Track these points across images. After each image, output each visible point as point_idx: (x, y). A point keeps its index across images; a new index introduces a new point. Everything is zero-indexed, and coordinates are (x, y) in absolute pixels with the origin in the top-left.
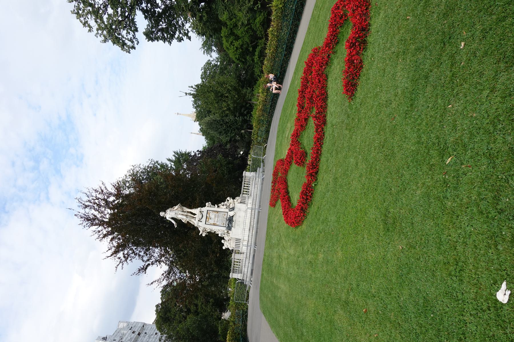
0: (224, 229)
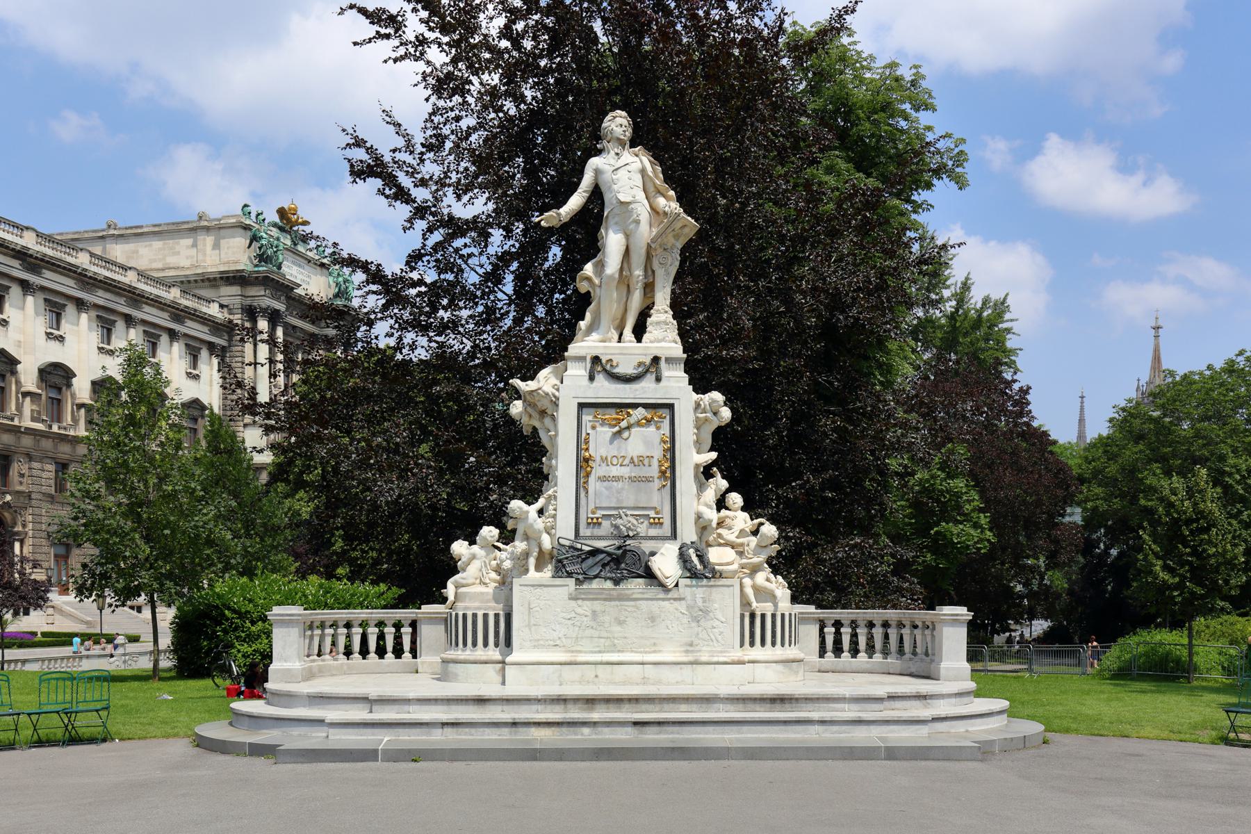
0: (565, 530)
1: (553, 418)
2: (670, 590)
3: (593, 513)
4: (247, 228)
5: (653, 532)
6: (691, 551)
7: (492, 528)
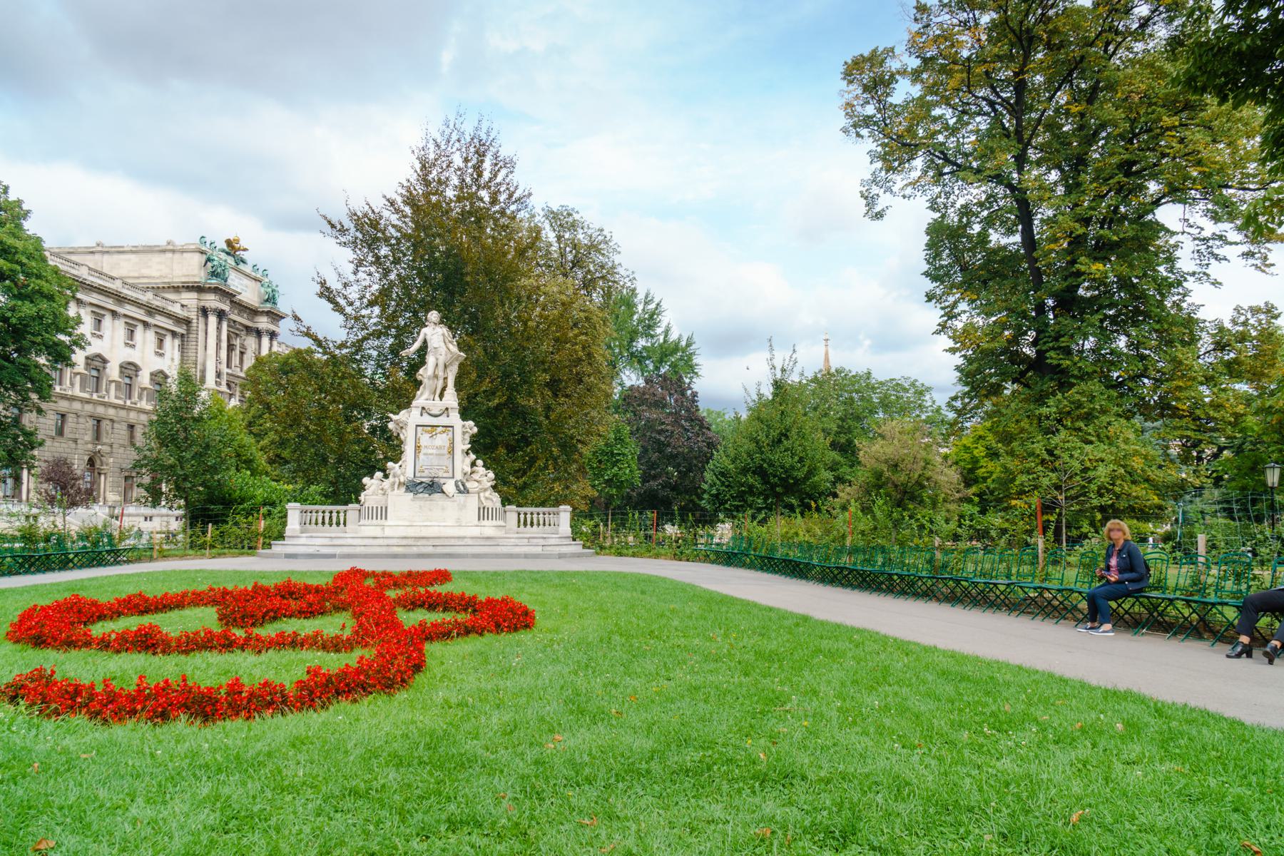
0: (410, 474)
4: (202, 253)
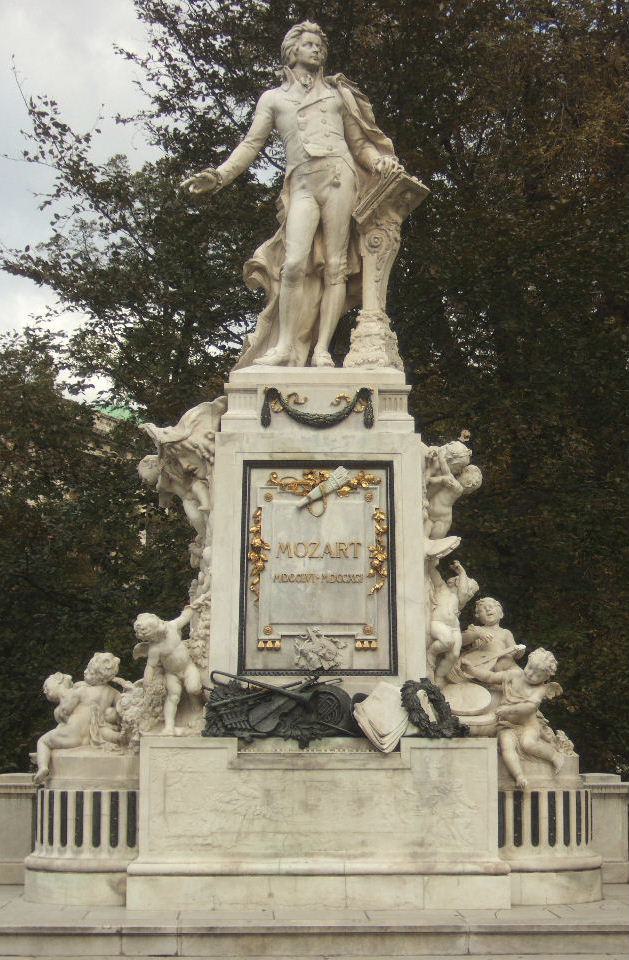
1: (207, 486)
2: (386, 755)
3: (267, 632)
5: (362, 661)
6: (421, 693)
7: (107, 655)
